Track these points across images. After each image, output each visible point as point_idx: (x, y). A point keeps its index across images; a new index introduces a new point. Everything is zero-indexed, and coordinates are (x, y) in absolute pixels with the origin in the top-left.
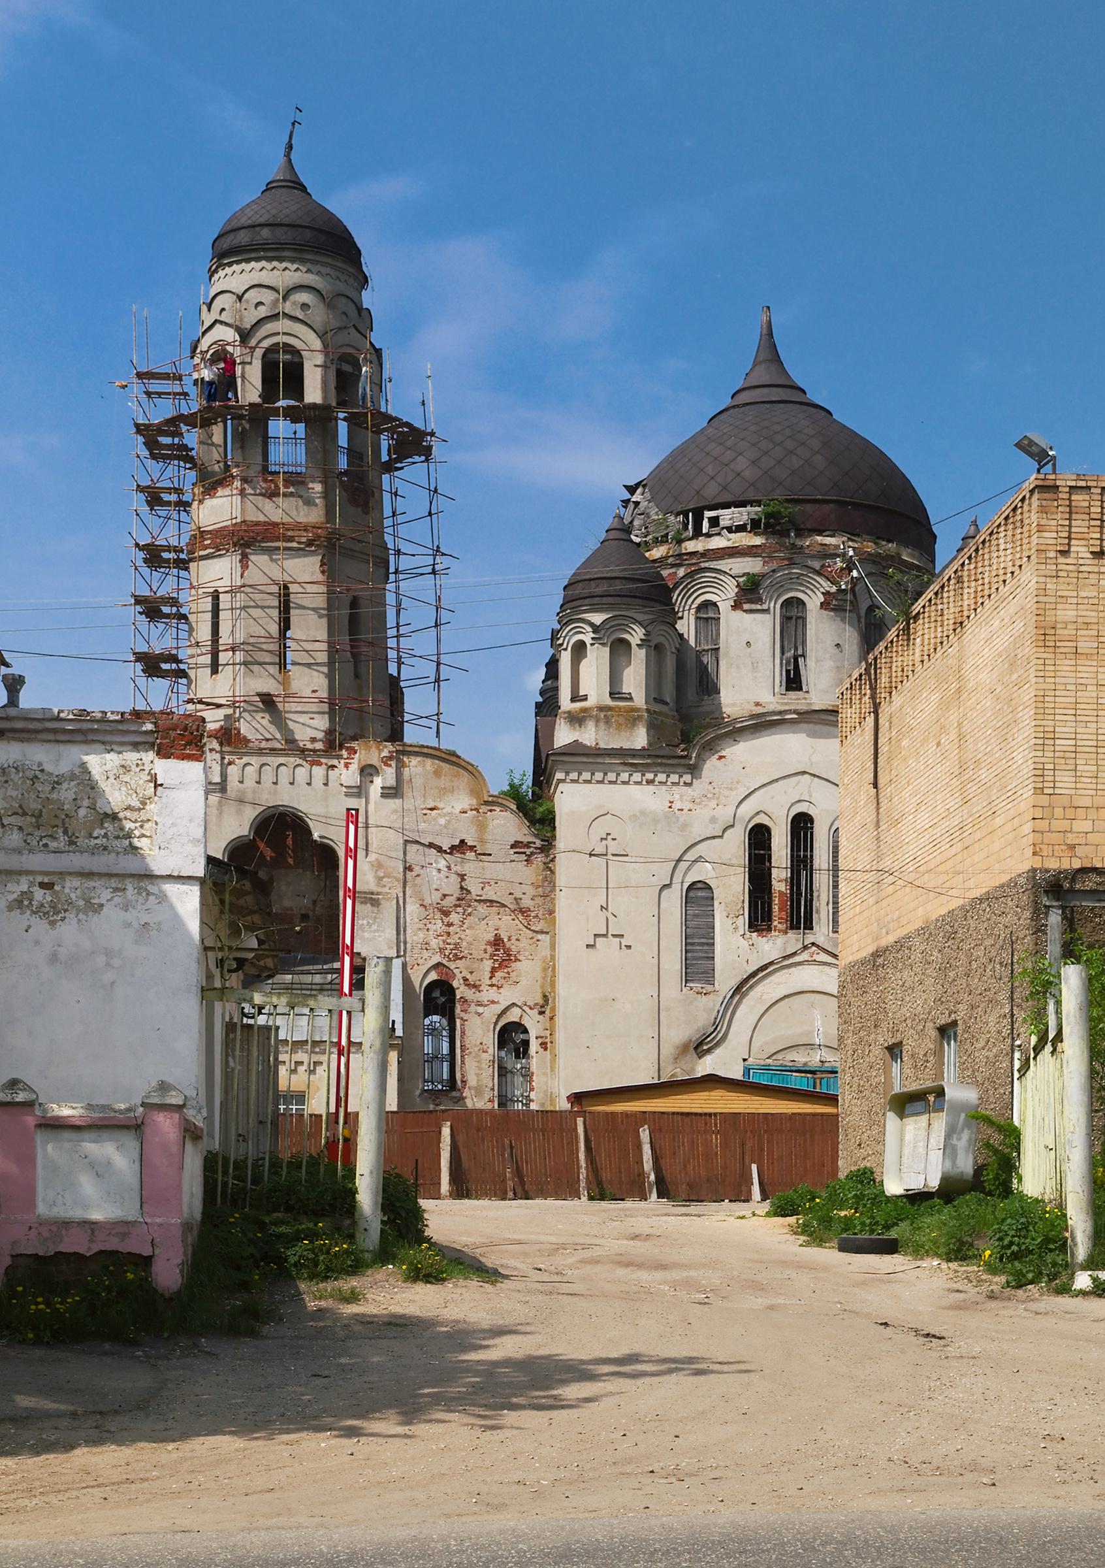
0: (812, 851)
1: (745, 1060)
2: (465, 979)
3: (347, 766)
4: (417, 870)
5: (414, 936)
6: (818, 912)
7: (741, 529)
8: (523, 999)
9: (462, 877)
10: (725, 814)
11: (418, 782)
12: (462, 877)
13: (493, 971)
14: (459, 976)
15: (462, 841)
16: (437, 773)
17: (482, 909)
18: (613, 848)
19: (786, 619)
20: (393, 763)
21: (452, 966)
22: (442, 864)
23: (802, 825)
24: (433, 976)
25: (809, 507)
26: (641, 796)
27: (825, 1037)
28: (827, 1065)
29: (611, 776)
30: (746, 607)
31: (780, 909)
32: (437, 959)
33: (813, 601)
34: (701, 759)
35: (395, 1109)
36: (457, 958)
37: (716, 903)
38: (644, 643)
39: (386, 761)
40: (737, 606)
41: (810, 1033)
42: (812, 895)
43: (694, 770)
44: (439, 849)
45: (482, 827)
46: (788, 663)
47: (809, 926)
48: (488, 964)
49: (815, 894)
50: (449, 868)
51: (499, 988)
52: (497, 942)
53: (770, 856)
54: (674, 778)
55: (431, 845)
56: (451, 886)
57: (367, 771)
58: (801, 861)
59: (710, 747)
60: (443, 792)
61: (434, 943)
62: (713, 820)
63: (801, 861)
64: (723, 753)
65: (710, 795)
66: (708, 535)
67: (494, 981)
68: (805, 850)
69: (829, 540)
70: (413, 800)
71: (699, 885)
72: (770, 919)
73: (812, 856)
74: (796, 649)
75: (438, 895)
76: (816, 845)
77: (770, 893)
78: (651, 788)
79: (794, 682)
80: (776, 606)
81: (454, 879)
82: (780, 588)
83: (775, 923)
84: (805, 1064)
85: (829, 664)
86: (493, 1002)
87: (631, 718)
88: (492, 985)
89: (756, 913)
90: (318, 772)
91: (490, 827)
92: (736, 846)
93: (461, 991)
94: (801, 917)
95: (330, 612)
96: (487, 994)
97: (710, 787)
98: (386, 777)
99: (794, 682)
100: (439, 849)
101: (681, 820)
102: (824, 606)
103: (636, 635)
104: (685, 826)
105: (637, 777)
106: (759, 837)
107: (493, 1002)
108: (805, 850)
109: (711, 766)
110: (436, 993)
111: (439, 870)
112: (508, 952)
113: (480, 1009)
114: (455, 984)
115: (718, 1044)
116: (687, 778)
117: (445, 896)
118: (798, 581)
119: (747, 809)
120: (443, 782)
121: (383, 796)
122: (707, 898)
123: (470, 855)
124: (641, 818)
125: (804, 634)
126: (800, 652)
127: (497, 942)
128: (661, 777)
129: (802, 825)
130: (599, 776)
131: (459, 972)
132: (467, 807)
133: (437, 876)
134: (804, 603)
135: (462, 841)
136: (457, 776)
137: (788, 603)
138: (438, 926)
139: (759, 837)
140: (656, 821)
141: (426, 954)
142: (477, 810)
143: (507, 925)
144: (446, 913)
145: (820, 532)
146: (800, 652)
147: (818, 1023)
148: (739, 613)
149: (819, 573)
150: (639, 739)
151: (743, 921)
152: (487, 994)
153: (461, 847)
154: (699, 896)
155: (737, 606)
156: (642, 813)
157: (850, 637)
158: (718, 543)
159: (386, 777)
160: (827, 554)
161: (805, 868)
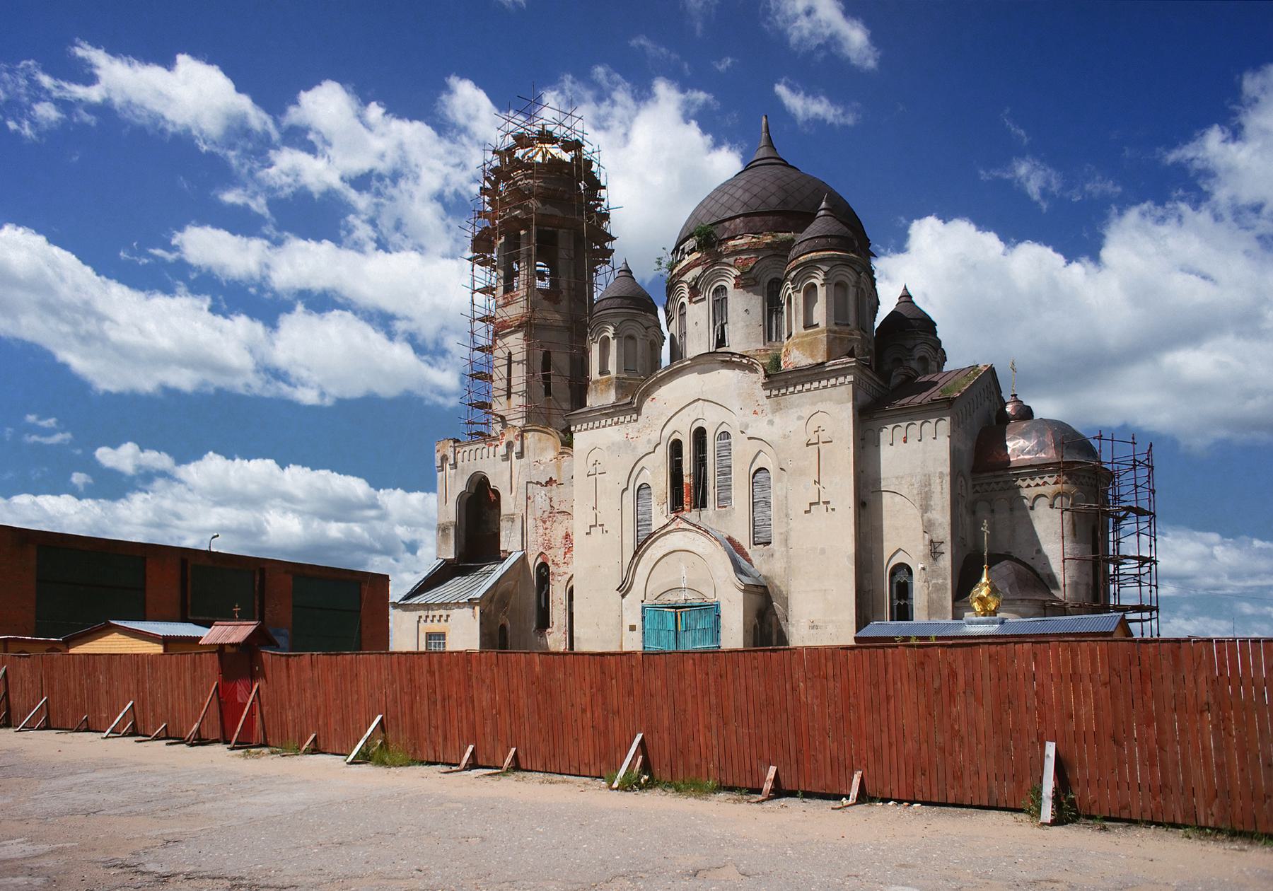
5: (531, 537)
7: (693, 250)
10: (655, 437)
11: (531, 448)
16: (540, 440)
17: (560, 517)
19: (716, 302)
23: (700, 436)
24: (540, 560)
25: (727, 224)
29: (597, 423)
32: (541, 550)
33: (730, 284)
34: (641, 402)
35: (740, 646)
38: (616, 336)
40: (690, 301)
43: (638, 411)
45: (559, 468)
47: (704, 505)
48: (563, 550)
54: (628, 418)
57: (510, 445)
58: (700, 462)
59: (647, 393)
60: (543, 450)
61: (540, 540)
63: (700, 462)
64: (653, 396)
66: (680, 261)
69: (741, 241)
70: (529, 458)
79: (721, 342)
82: (709, 282)
85: (741, 324)
87: (608, 384)
90: (491, 449)
92: (663, 453)
95: (528, 361)
98: (517, 448)
99: (721, 342)
102: (736, 286)
103: (610, 332)
104: (634, 449)
105: (609, 421)
106: (676, 447)
109: (647, 406)
115: (627, 591)
116: (635, 416)
118: (720, 274)
119: (667, 432)
128: (622, 419)
129: (700, 436)
130: (591, 424)
137: (716, 291)
138: (541, 531)
139: (676, 447)
144: (544, 522)
145: (733, 238)
147: (683, 573)
150: (611, 397)
152: (563, 568)
157: (755, 303)
158: (684, 263)
159: (517, 448)
160: (736, 252)
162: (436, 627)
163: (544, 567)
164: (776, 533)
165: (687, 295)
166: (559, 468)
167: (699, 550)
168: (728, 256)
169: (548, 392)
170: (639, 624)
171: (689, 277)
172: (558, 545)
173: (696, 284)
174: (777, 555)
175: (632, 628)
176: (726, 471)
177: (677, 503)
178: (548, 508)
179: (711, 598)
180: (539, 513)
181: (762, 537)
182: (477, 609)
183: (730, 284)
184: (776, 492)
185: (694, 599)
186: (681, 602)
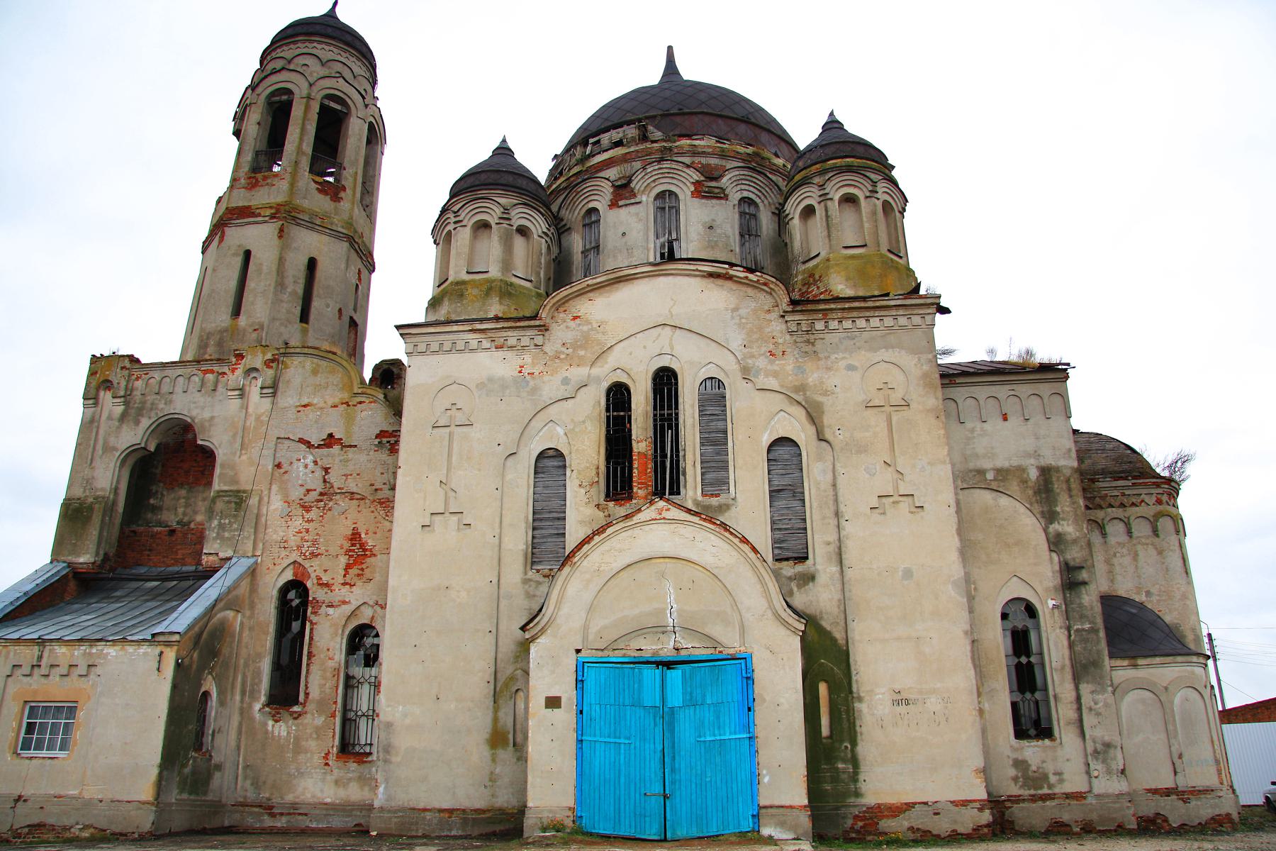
0: (677, 408)
1: (578, 651)
2: (319, 578)
3: (233, 371)
4: (285, 467)
6: (684, 474)
8: (375, 598)
9: (326, 470)
12: (326, 470)
13: (348, 567)
14: (313, 575)
15: (331, 435)
17: (343, 503)
18: (460, 418)
20: (274, 365)
21: (307, 564)
22: (310, 459)
23: (665, 381)
24: (289, 576)
26: (488, 363)
27: (679, 615)
28: (683, 652)
30: (621, 203)
31: (643, 472)
32: (295, 556)
33: (685, 192)
36: (314, 555)
37: (568, 472)
39: (268, 364)
40: (614, 204)
41: (663, 611)
42: (678, 456)
44: (309, 444)
45: (350, 420)
46: (662, 246)
47: (675, 490)
48: (343, 560)
49: (681, 454)
50: (315, 463)
51: (351, 586)
52: (355, 537)
53: (630, 417)
55: (301, 441)
56: (316, 483)
61: (294, 541)
62: (566, 381)
65: (562, 356)
67: (348, 579)
68: (670, 408)
70: (288, 399)
71: (551, 453)
72: (631, 488)
73: (677, 414)
74: (670, 233)
75: (303, 490)
76: (680, 400)
77: (631, 456)
78: (501, 354)
80: (647, 199)
81: (319, 473)
83: (635, 490)
84: (655, 653)
86: (344, 602)
88: (344, 584)
89: (615, 482)
91: (358, 418)
93: (315, 592)
94: (667, 483)
96: (341, 593)
97: (564, 349)
100: (309, 444)
101: (532, 383)
104: (535, 390)
107: (344, 602)
108: (670, 408)
110: (292, 595)
111: (306, 466)
112: (362, 546)
113: (331, 611)
114: (309, 584)
117: (308, 491)
120: (320, 379)
121: (262, 395)
122: (559, 467)
123: (337, 448)
124: (489, 386)
125: (678, 220)
126: (674, 236)
127: (355, 537)
129: (665, 381)
131: (314, 568)
132: (337, 401)
133: (304, 470)
134: (676, 195)
135: (331, 435)
136: (332, 372)
138: (298, 523)
139: (618, 396)
140: (504, 387)
141: (284, 553)
142: (347, 404)
143: (362, 518)
146: (674, 236)
147: (671, 599)
148: (615, 211)
149: (688, 166)
151: (599, 492)
153: (330, 441)
154: (550, 462)
155: (614, 204)
156: (491, 380)
160: (694, 152)
161: (670, 427)
162: (54, 688)
163: (297, 585)
164: (820, 540)
165: (608, 197)
166: (350, 420)
167: (708, 559)
168: (681, 154)
169: (304, 317)
170: (567, 691)
171: (612, 173)
172: (334, 549)
173: (630, 181)
174: (822, 579)
175: (553, 702)
176: (716, 440)
177: (618, 485)
178: (319, 487)
179: (731, 642)
180: (297, 493)
181: (793, 544)
182: (171, 656)
183: (685, 192)
184: (815, 475)
185: (692, 647)
186: (667, 652)
